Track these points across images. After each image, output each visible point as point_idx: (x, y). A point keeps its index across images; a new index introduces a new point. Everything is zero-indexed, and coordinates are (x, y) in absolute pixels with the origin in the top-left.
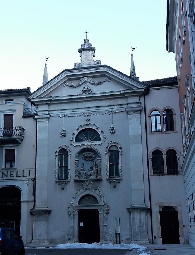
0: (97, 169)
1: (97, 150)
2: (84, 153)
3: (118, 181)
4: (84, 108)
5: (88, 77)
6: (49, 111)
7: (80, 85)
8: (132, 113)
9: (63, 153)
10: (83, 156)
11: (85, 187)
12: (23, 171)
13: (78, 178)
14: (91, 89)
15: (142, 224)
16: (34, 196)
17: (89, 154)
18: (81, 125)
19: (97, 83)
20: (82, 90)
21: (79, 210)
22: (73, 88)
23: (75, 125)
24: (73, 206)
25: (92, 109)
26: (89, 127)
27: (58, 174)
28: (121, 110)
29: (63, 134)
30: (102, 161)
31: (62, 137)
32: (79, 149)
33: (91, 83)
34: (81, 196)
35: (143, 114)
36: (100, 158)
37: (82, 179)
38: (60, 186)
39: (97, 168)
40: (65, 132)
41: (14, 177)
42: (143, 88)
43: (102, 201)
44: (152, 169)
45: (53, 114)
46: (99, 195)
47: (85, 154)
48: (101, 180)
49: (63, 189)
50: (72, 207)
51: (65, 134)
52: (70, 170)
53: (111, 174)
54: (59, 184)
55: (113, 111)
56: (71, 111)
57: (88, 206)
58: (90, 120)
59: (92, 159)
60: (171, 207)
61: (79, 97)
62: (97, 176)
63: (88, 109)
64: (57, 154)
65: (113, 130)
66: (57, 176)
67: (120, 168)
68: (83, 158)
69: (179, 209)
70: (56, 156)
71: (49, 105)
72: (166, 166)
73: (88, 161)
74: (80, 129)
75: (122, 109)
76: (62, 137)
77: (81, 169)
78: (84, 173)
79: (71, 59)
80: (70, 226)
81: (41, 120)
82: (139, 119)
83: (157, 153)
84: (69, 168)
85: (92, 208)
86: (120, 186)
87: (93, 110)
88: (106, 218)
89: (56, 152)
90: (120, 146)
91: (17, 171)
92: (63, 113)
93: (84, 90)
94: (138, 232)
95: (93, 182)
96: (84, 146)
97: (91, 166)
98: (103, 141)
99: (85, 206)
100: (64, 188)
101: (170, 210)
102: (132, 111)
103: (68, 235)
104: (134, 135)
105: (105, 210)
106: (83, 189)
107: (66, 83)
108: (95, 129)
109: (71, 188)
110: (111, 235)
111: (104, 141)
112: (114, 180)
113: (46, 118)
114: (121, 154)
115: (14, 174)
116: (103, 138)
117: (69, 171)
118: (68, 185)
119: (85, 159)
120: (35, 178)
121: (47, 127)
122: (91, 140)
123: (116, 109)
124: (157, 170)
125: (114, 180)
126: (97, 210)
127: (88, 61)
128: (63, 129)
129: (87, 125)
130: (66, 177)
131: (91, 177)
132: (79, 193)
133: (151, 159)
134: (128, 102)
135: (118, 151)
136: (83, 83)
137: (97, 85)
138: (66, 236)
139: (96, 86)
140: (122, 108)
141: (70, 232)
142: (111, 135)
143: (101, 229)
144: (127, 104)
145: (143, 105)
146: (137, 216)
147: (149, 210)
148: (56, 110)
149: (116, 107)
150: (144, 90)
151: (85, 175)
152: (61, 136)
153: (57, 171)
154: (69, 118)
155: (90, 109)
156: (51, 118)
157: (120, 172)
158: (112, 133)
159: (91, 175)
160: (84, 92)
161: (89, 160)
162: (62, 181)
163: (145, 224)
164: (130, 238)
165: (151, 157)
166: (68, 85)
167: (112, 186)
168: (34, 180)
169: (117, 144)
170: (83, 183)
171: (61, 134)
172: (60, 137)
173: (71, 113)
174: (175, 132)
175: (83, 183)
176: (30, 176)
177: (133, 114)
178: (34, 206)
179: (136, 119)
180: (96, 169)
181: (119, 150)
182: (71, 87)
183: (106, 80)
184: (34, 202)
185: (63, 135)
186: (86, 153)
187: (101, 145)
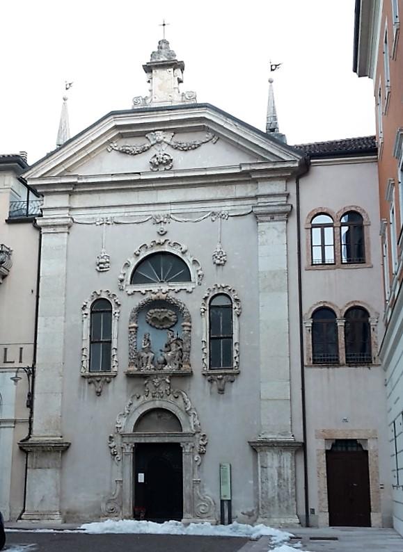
0: (181, 349)
2: (152, 311)
3: (230, 378)
4: (154, 204)
6: (71, 209)
7: (144, 151)
8: (268, 218)
9: (101, 309)
10: (149, 318)
11: (151, 390)
12: (6, 349)
13: (136, 369)
14: (172, 160)
15: (284, 480)
18: (145, 245)
19: (185, 145)
20: (151, 162)
21: (135, 444)
25: (173, 207)
26: (163, 250)
27: (88, 358)
29: (102, 265)
30: (192, 330)
32: (138, 301)
33: (172, 146)
34: (141, 411)
35: (293, 220)
36: (189, 324)
37: (143, 371)
38: (92, 385)
39: (181, 347)
40: (108, 260)
43: (190, 423)
44: (311, 350)
45: (79, 216)
46: (184, 409)
48: (189, 375)
49: (99, 394)
50: (119, 438)
51: (107, 264)
53: (214, 362)
54: (89, 383)
56: (123, 210)
57: (157, 435)
58: (166, 232)
62: (180, 365)
63: (163, 207)
64: (88, 311)
66: (86, 364)
67: (235, 348)
68: (148, 322)
69: (370, 447)
70: (85, 316)
71: (70, 195)
73: (160, 331)
74: (144, 254)
75: (245, 209)
77: (143, 349)
79: (128, 88)
80: (113, 481)
81: (51, 230)
82: (282, 232)
83: (323, 314)
84: (114, 345)
85: (167, 440)
86: (234, 389)
88: (198, 463)
89: (84, 307)
90: (236, 297)
92: (104, 216)
93: (156, 160)
94: (274, 497)
95: (170, 380)
96: (152, 295)
97: (166, 342)
98: (197, 283)
99: (150, 435)
100: (101, 392)
101: (349, 449)
102: (266, 214)
103: (109, 502)
104: (270, 272)
105: (197, 446)
106: (147, 396)
107: (111, 145)
109: (118, 390)
110: (211, 504)
112: (221, 374)
113: (64, 225)
114: (238, 316)
116: (197, 276)
117: (113, 352)
118: (110, 386)
120: (33, 367)
122: (168, 279)
123: (229, 208)
124: (323, 355)
125: (221, 376)
126: (178, 444)
127: (166, 94)
128: (104, 252)
129: (159, 244)
130: (107, 366)
132: (136, 404)
133: (308, 328)
134: (258, 194)
136: (152, 145)
137: (186, 150)
138: (103, 506)
140: (245, 207)
141: (113, 496)
142: (217, 269)
143: (187, 489)
144: (256, 197)
145: (293, 201)
146: (271, 460)
147: (301, 448)
148: (86, 208)
150: (297, 165)
151: (152, 363)
152: (98, 269)
153: (86, 353)
155: (168, 207)
156: (75, 226)
157: (235, 358)
158: (219, 265)
159: (165, 363)
161: (161, 327)
162: (97, 374)
163: (290, 480)
164: (253, 511)
165: (308, 323)
166: (117, 148)
167: (215, 390)
168: (31, 372)
170: (146, 382)
171: (98, 265)
172: (96, 272)
173: (122, 214)
174: (368, 266)
175: (146, 382)
176: (20, 362)
177: (269, 221)
178: (30, 433)
179: (276, 233)
180: (179, 348)
181: (235, 305)
182: (125, 153)
183: (207, 140)
184: (30, 422)
185: (102, 268)
186: (156, 310)
187: (191, 292)
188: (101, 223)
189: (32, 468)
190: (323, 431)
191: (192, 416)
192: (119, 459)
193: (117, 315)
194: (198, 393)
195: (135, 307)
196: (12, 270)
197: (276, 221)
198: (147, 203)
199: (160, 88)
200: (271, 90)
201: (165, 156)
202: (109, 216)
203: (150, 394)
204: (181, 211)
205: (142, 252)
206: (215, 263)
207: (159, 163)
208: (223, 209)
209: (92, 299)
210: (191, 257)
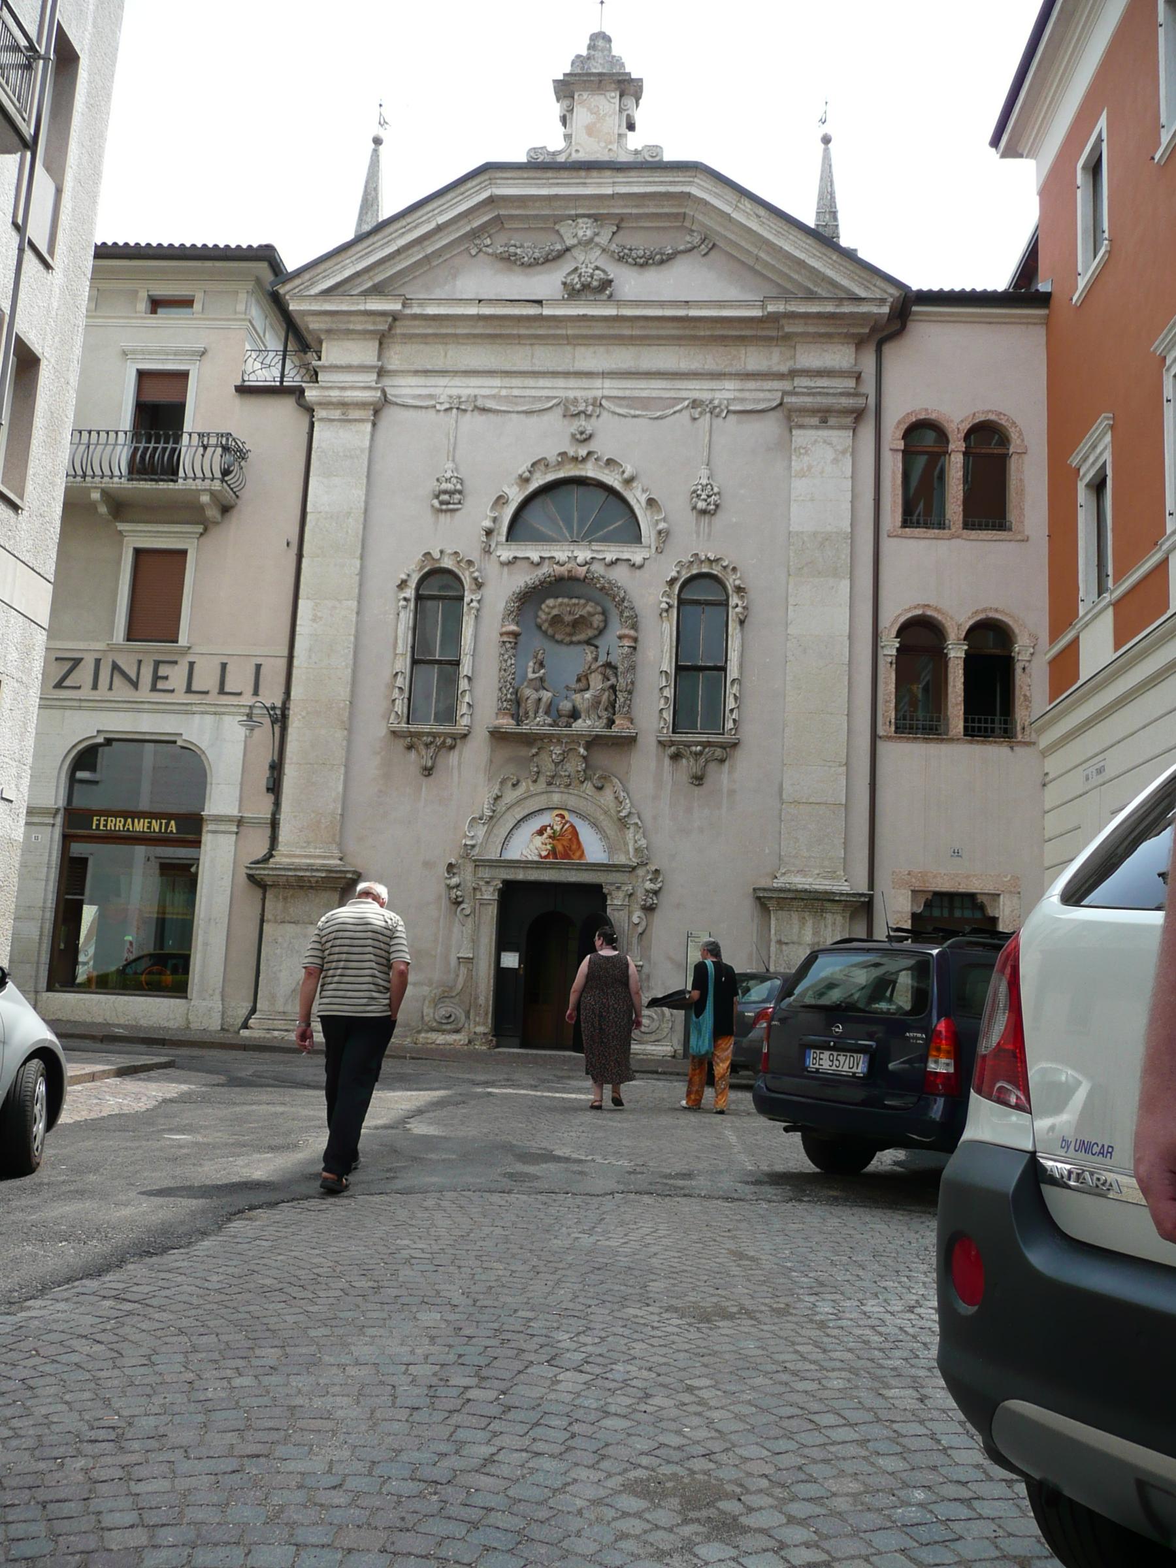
1: (619, 588)
2: (550, 602)
3: (719, 752)
4: (567, 374)
5: (594, 229)
7: (552, 258)
8: (815, 421)
9: (438, 591)
10: (544, 617)
11: (543, 769)
12: (224, 666)
14: (611, 281)
16: (270, 798)
19: (641, 253)
20: (564, 284)
21: (506, 883)
22: (516, 268)
23: (508, 452)
24: (475, 861)
25: (608, 383)
26: (583, 473)
27: (406, 695)
28: (758, 401)
29: (445, 497)
31: (442, 511)
32: (523, 579)
36: (632, 633)
38: (413, 755)
39: (613, 680)
40: (459, 487)
41: (173, 691)
42: (882, 301)
43: (626, 844)
44: (893, 705)
46: (613, 812)
47: (553, 608)
48: (628, 742)
49: (428, 771)
50: (470, 867)
51: (457, 496)
52: (469, 679)
53: (682, 716)
55: (716, 402)
56: (497, 382)
58: (591, 436)
59: (582, 637)
60: (970, 899)
61: (547, 311)
62: (608, 718)
63: (585, 382)
64: (410, 593)
65: (709, 496)
67: (733, 690)
68: (539, 627)
70: (403, 603)
72: (961, 699)
75: (764, 400)
76: (442, 511)
78: (544, 700)
82: (844, 452)
83: (920, 638)
84: (465, 668)
87: (609, 387)
88: (640, 930)
89: (403, 585)
90: (737, 582)
91: (192, 664)
92: (455, 392)
93: (577, 280)
95: (586, 749)
100: (431, 769)
101: (957, 914)
102: (813, 412)
104: (815, 534)
105: (640, 894)
106: (535, 781)
107: (477, 242)
108: (618, 486)
109: (470, 772)
111: (659, 551)
112: (697, 744)
113: (362, 405)
114: (742, 622)
115: (176, 676)
116: (653, 534)
117: (463, 684)
118: (453, 757)
121: (362, 451)
122: (588, 536)
123: (730, 395)
124: (917, 716)
126: (598, 888)
127: (603, 144)
129: (575, 459)
130: (448, 714)
131: (580, 721)
132: (510, 796)
134: (798, 367)
135: (727, 605)
137: (642, 266)
138: (428, 1011)
139: (635, 268)
144: (793, 374)
145: (869, 387)
148: (416, 372)
149: (730, 385)
150: (886, 310)
151: (546, 713)
154: (480, 419)
155: (598, 383)
157: (732, 711)
158: (704, 512)
159: (575, 715)
160: (573, 293)
161: (568, 639)
165: (890, 647)
166: (490, 250)
168: (281, 718)
169: (725, 568)
171: (437, 497)
174: (1019, 537)
175: (534, 751)
176: (256, 693)
177: (816, 428)
179: (830, 454)
181: (734, 600)
184: (274, 824)
186: (560, 600)
187: (641, 567)
188: (447, 406)
189: (276, 922)
190: (909, 874)
191: (632, 830)
192: (467, 912)
193: (474, 604)
194: (648, 776)
195: (518, 591)
196: (245, 495)
197: (832, 428)
198: (551, 369)
199: (590, 130)
200: (826, 153)
201: (597, 272)
202: (465, 392)
203: (542, 779)
204: (627, 393)
205: (537, 475)
206: (694, 508)
207: (583, 285)
208: (718, 395)
209: (421, 568)
210: (644, 491)
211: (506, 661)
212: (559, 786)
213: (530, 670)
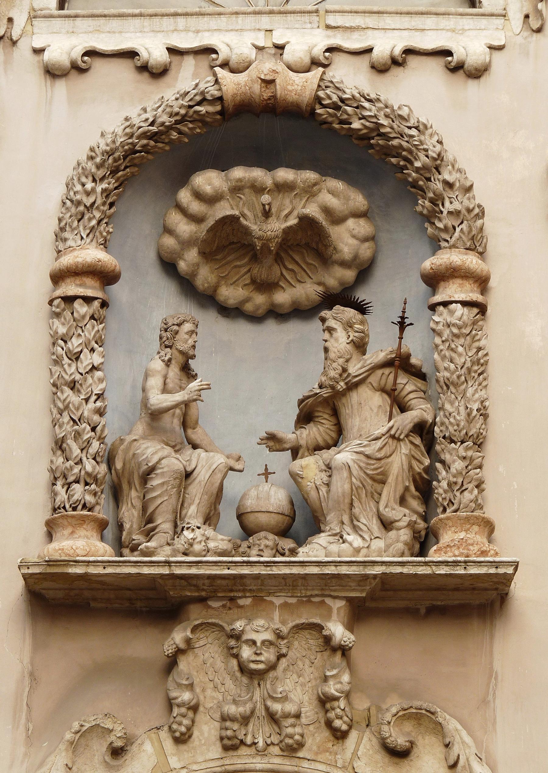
0: (423, 431)
2: (208, 180)
10: (185, 228)
17: (282, 188)
30: (495, 303)
32: (117, 110)
37: (162, 556)
47: (211, 200)
59: (307, 290)
68: (168, 266)
73: (242, 330)
77: (155, 416)
78: (202, 475)
95: (350, 627)
97: (308, 379)
119: (205, 277)
131: (322, 539)
151: (211, 519)
159: (301, 521)
161: (260, 300)
170: (178, 636)
186: (239, 173)
187: (477, 73)
203: (207, 731)
211: (76, 357)
212: (262, 753)
213: (155, 382)
